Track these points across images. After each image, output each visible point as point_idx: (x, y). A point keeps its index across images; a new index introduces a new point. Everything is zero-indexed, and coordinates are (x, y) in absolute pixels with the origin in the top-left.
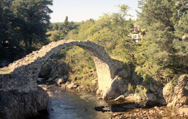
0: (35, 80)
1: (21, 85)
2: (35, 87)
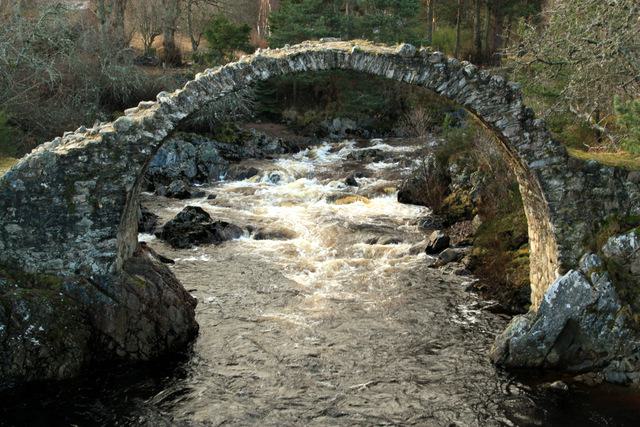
0: (103, 225)
1: (39, 244)
2: (103, 259)
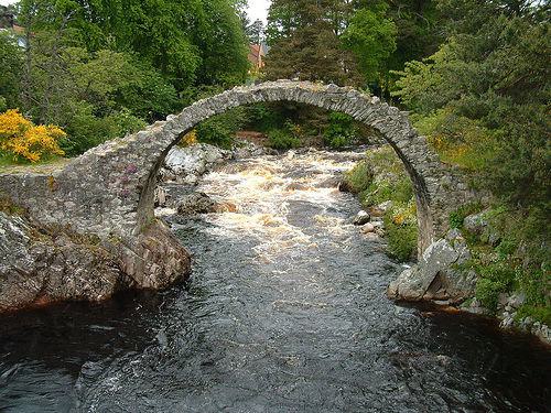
0: (128, 204)
